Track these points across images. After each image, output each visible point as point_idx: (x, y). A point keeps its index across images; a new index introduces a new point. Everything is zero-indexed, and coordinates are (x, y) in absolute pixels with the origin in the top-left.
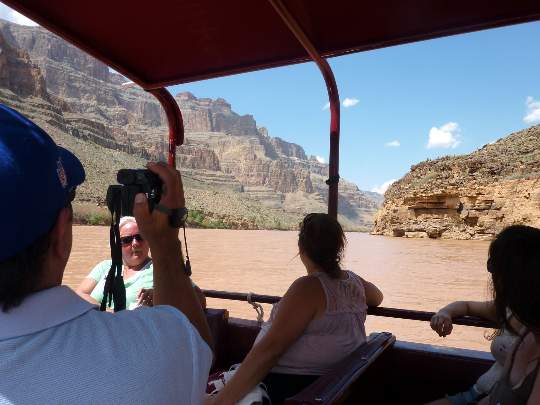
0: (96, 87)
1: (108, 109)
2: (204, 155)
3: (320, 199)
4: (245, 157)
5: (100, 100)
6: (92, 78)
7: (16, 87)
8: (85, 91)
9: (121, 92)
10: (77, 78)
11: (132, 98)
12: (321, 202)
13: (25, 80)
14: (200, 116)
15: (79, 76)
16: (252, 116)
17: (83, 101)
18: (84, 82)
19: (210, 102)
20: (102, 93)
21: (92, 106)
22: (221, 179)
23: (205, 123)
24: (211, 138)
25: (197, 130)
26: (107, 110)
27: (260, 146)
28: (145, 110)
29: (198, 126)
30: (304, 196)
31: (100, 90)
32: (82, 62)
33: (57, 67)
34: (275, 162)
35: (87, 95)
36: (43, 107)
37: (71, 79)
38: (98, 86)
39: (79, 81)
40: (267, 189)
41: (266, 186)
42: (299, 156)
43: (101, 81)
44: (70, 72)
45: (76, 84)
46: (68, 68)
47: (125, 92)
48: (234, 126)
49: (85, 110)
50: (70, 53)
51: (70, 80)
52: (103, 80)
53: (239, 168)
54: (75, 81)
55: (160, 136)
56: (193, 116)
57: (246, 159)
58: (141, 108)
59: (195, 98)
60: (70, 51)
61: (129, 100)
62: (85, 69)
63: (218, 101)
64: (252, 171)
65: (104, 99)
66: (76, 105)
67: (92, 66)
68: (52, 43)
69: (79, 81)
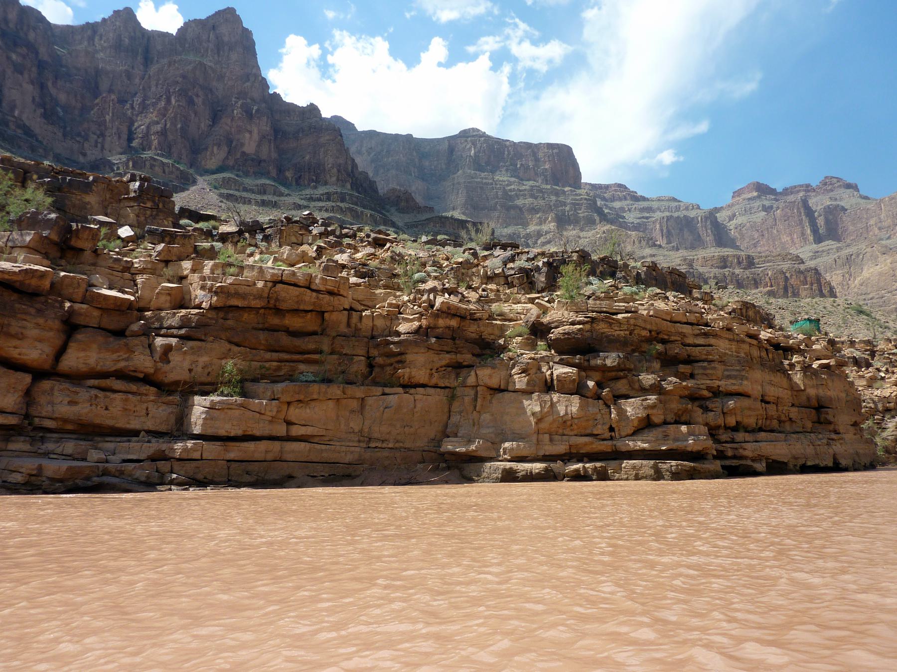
0: (556, 201)
1: (582, 234)
2: (792, 281)
5: (562, 221)
6: (549, 187)
7: (289, 174)
8: (534, 210)
9: (625, 212)
10: (521, 191)
11: (643, 217)
13: (307, 158)
14: (786, 218)
15: (524, 187)
17: (532, 228)
18: (532, 196)
19: (807, 191)
20: (567, 208)
21: (547, 233)
24: (816, 255)
26: (579, 237)
28: (668, 231)
29: (785, 238)
31: (565, 204)
32: (531, 164)
33: (484, 181)
35: (538, 216)
36: (329, 199)
37: (511, 196)
38: (561, 198)
39: (524, 195)
43: (566, 189)
44: (508, 185)
45: (519, 202)
46: (505, 179)
47: (630, 210)
48: (872, 222)
49: (536, 243)
50: (509, 154)
51: (507, 196)
52: (570, 186)
54: (517, 196)
55: (685, 260)
56: (770, 221)
58: (662, 230)
59: (773, 191)
60: (509, 151)
61: (638, 221)
62: (536, 174)
63: (825, 184)
65: (572, 218)
66: (519, 236)
67: (547, 167)
68: (479, 145)
69: (524, 195)
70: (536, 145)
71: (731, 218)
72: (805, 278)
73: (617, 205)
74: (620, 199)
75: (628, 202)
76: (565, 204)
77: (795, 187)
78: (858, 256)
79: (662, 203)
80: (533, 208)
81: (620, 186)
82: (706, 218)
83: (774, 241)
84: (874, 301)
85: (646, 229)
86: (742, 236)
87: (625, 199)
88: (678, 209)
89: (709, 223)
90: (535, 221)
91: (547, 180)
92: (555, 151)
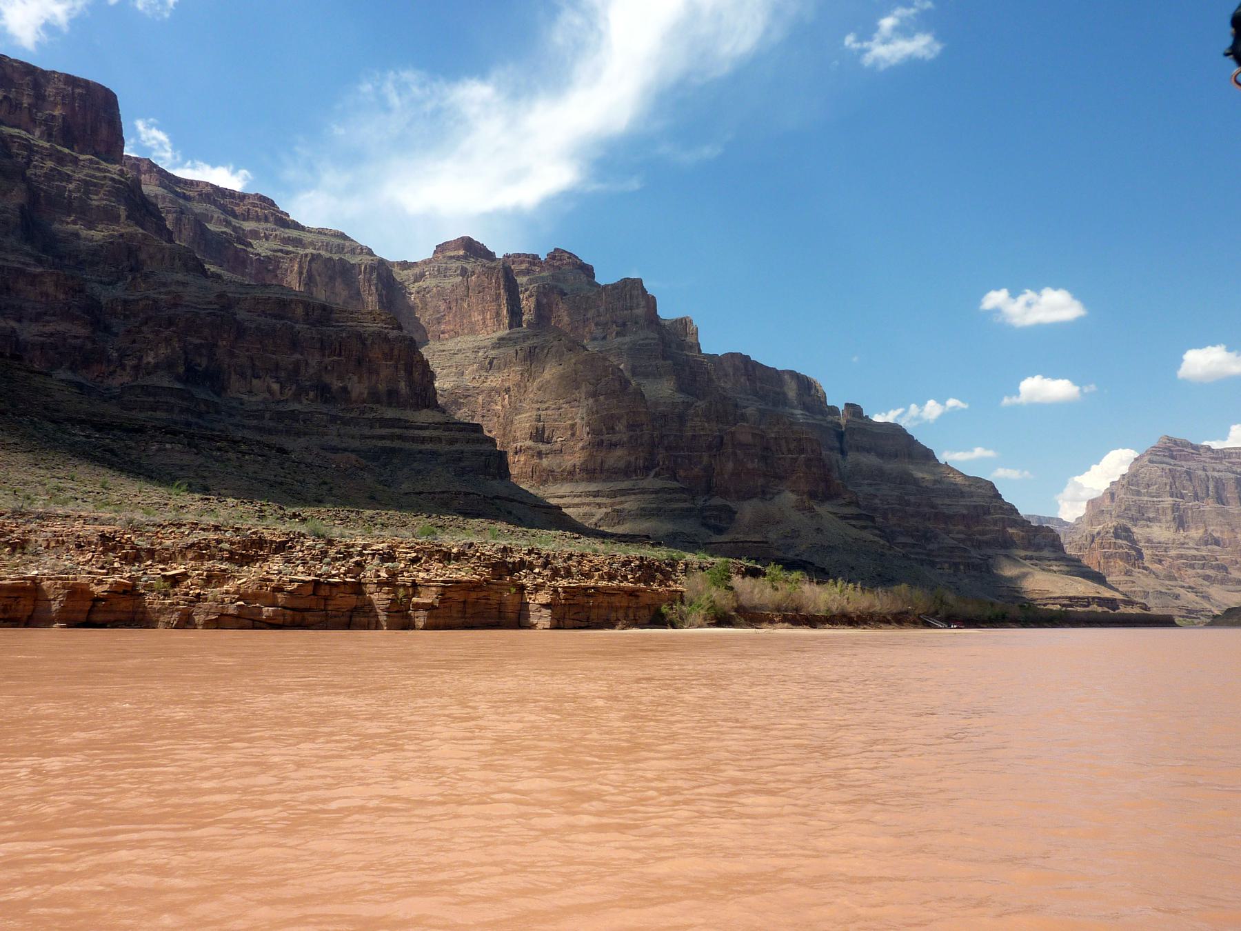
3: (858, 517)
4: (591, 388)
11: (281, 251)
12: (864, 528)
14: (482, 289)
16: (639, 282)
20: (71, 186)
22: (427, 433)
23: (493, 306)
25: (473, 332)
27: (660, 362)
28: (310, 277)
29: (477, 317)
30: (801, 508)
32: (26, 102)
34: (701, 404)
38: (67, 170)
40: (659, 484)
41: (656, 475)
42: (806, 407)
47: (267, 238)
48: (590, 315)
53: (573, 426)
56: (461, 291)
57: (594, 395)
58: (301, 273)
62: (33, 121)
64: (611, 430)
65: (76, 204)
67: (56, 113)
70: (44, 73)
71: (418, 278)
72: (392, 350)
73: (249, 226)
74: (258, 219)
75: (269, 225)
76: (69, 179)
77: (519, 255)
78: (543, 349)
79: (324, 238)
81: (263, 199)
82: (372, 268)
83: (462, 317)
84: (549, 412)
85: (278, 267)
86: (425, 304)
87: (266, 220)
88: (341, 249)
89: (374, 276)
91: (50, 135)
92: (78, 91)
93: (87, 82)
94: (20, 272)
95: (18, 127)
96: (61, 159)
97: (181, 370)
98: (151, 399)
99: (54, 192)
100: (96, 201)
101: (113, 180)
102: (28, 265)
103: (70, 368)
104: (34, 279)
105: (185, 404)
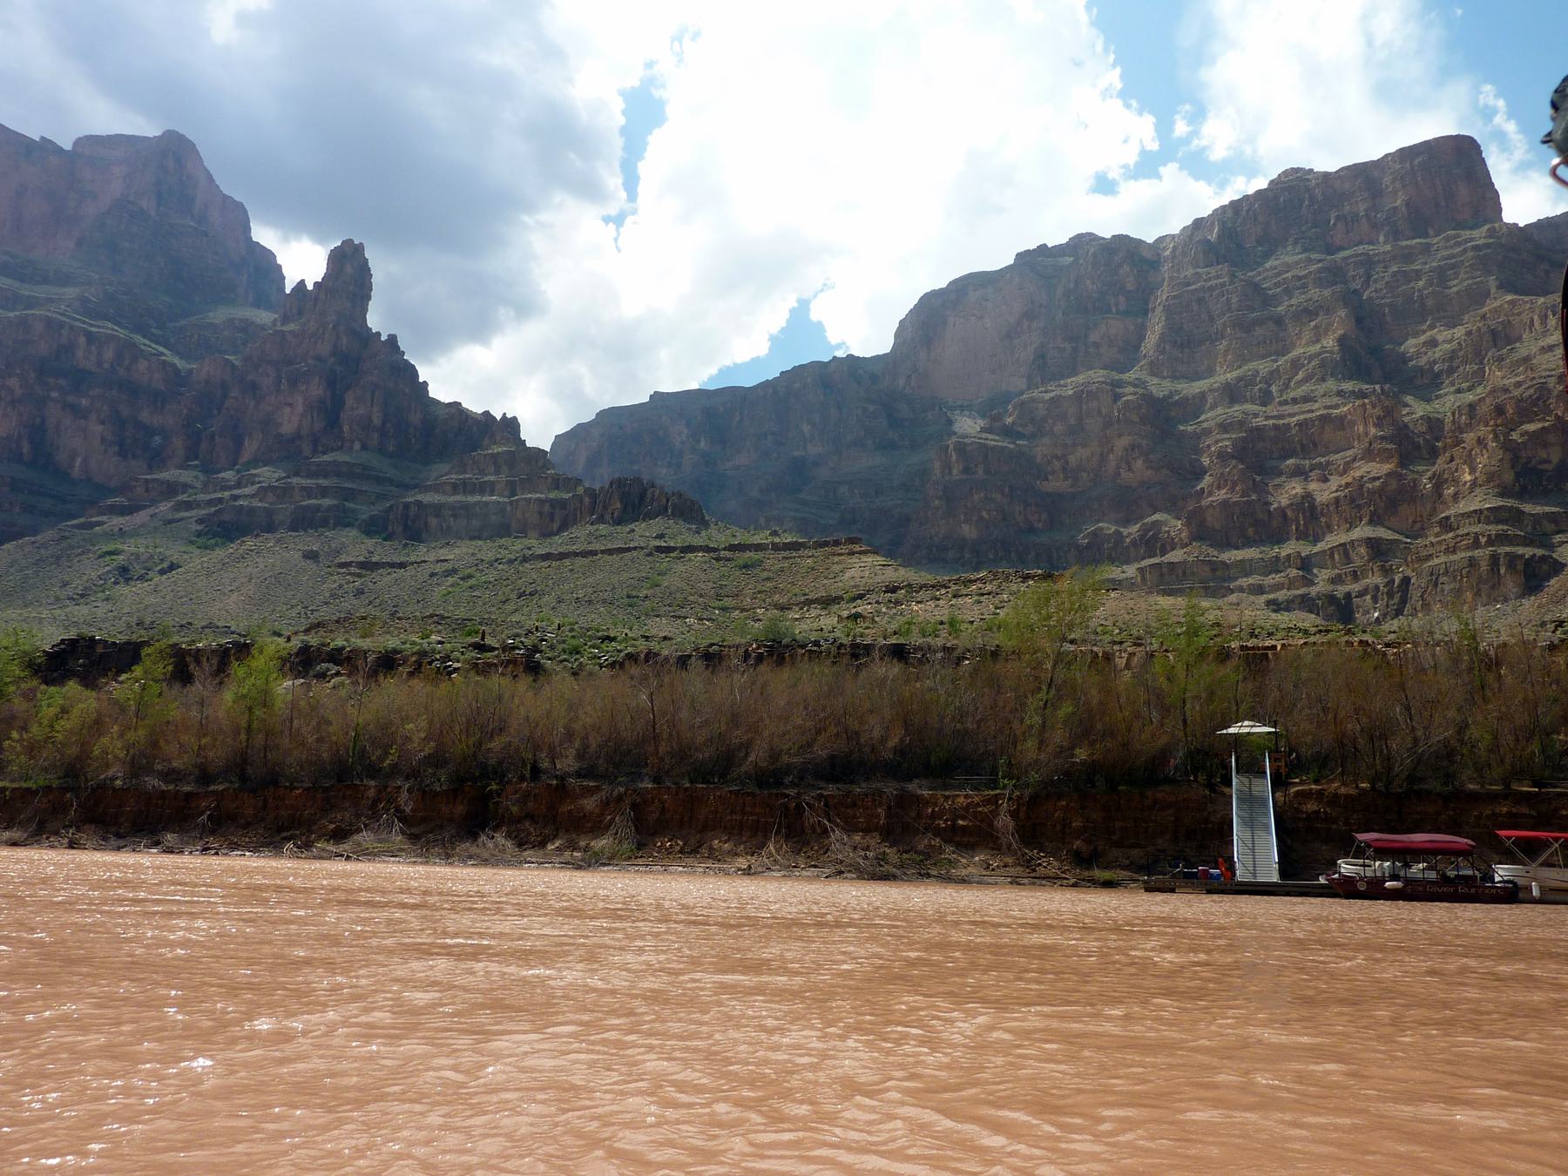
20: (1421, 283)
54: (1288, 292)
65: (1430, 303)
76: (1418, 275)
80: (1306, 310)
90: (1307, 335)
93: (1426, 142)
94: (1324, 419)
95: (1361, 243)
96: (1408, 257)
97: (1509, 477)
98: (1451, 535)
99: (1400, 300)
100: (1455, 286)
101: (1476, 248)
102: (1336, 406)
103: (1371, 522)
104: (1341, 422)
105: (1494, 529)
